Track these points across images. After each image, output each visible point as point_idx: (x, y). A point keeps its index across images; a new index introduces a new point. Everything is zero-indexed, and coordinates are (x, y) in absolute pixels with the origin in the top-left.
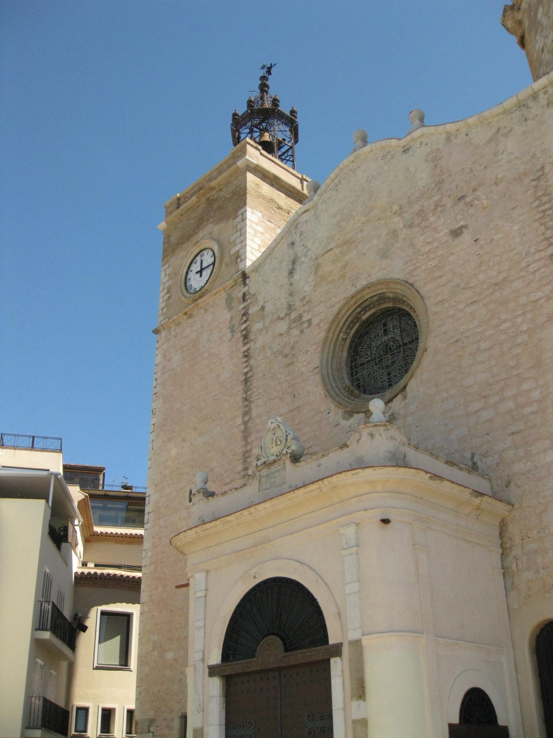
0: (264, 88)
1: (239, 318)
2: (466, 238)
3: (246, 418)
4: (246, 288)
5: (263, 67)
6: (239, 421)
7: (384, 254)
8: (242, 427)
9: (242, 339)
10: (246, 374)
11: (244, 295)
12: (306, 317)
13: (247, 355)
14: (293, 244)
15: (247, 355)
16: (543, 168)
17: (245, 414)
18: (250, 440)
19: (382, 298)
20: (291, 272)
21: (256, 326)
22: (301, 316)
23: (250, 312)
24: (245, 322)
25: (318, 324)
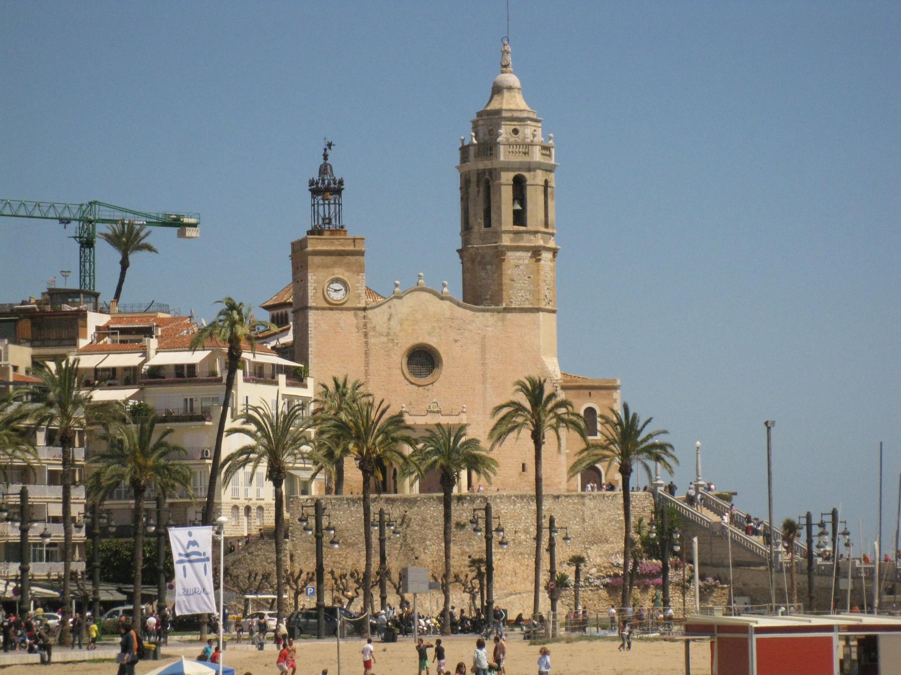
0: (326, 157)
1: (361, 325)
2: (459, 344)
3: (367, 368)
4: (365, 314)
5: (325, 139)
6: (363, 368)
7: (430, 334)
8: (364, 371)
9: (363, 335)
10: (366, 351)
11: (364, 317)
12: (395, 341)
13: (366, 343)
14: (390, 307)
15: (366, 343)
16: (485, 336)
17: (365, 367)
18: (369, 377)
19: (425, 348)
20: (389, 319)
21: (371, 333)
22: (393, 340)
23: (369, 326)
24: (366, 328)
25: (401, 347)
